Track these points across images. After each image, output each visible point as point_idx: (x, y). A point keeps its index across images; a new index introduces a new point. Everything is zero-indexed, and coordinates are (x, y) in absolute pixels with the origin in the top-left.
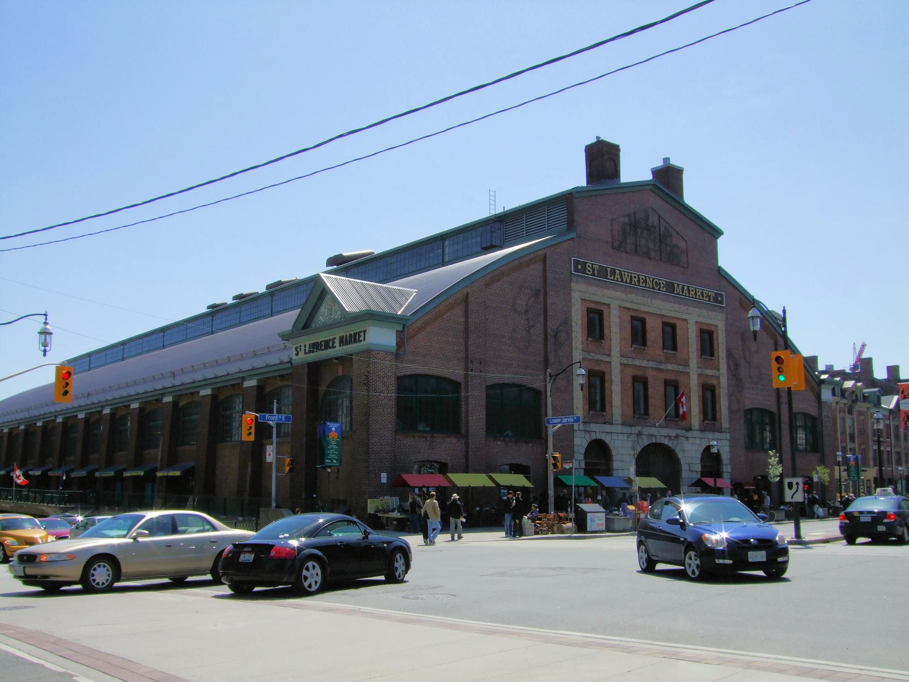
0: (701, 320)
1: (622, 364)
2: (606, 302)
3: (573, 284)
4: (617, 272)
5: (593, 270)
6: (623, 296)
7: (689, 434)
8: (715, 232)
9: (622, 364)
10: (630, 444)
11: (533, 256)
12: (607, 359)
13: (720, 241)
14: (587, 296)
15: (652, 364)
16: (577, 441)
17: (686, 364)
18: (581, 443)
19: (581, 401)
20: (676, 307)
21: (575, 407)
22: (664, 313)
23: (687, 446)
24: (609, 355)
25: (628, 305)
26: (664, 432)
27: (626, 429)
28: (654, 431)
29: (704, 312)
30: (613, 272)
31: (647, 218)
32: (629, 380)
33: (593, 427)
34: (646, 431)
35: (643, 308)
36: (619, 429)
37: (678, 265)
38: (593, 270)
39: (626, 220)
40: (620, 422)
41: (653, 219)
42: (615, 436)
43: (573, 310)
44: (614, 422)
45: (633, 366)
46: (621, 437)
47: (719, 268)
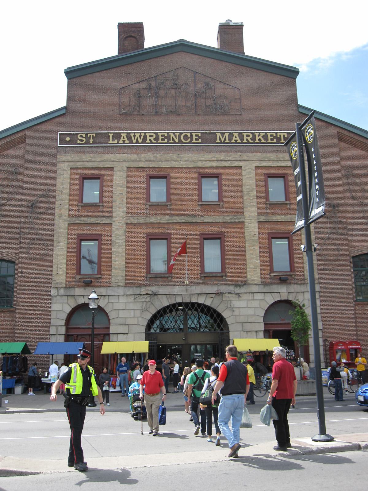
0: (264, 164)
1: (127, 224)
2: (109, 166)
3: (58, 156)
4: (124, 135)
5: (88, 138)
6: (134, 157)
7: (242, 290)
8: (291, 73)
9: (127, 224)
10: (138, 306)
11: (9, 139)
12: (107, 221)
13: (298, 79)
14: (79, 165)
15: (182, 219)
16: (55, 307)
17: (240, 212)
18: (61, 308)
19: (64, 267)
20: (222, 156)
21: (54, 273)
22: (200, 164)
23: (237, 303)
24: (111, 217)
25: (142, 164)
26: (197, 289)
27: (130, 291)
28: (177, 290)
29: (273, 156)
30: (117, 136)
31: (176, 78)
32: (142, 239)
33: (78, 291)
34: (162, 290)
35: (164, 165)
36: (121, 291)
37: (225, 114)
38: (88, 138)
39: (144, 85)
40: (122, 283)
41: (186, 77)
42: (112, 299)
43: (58, 179)
44: (112, 285)
45: (146, 224)
46: (122, 299)
47: (299, 106)
